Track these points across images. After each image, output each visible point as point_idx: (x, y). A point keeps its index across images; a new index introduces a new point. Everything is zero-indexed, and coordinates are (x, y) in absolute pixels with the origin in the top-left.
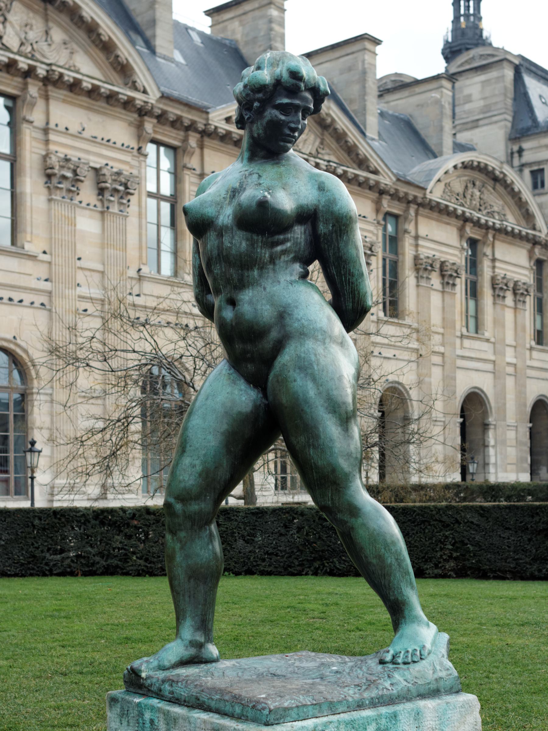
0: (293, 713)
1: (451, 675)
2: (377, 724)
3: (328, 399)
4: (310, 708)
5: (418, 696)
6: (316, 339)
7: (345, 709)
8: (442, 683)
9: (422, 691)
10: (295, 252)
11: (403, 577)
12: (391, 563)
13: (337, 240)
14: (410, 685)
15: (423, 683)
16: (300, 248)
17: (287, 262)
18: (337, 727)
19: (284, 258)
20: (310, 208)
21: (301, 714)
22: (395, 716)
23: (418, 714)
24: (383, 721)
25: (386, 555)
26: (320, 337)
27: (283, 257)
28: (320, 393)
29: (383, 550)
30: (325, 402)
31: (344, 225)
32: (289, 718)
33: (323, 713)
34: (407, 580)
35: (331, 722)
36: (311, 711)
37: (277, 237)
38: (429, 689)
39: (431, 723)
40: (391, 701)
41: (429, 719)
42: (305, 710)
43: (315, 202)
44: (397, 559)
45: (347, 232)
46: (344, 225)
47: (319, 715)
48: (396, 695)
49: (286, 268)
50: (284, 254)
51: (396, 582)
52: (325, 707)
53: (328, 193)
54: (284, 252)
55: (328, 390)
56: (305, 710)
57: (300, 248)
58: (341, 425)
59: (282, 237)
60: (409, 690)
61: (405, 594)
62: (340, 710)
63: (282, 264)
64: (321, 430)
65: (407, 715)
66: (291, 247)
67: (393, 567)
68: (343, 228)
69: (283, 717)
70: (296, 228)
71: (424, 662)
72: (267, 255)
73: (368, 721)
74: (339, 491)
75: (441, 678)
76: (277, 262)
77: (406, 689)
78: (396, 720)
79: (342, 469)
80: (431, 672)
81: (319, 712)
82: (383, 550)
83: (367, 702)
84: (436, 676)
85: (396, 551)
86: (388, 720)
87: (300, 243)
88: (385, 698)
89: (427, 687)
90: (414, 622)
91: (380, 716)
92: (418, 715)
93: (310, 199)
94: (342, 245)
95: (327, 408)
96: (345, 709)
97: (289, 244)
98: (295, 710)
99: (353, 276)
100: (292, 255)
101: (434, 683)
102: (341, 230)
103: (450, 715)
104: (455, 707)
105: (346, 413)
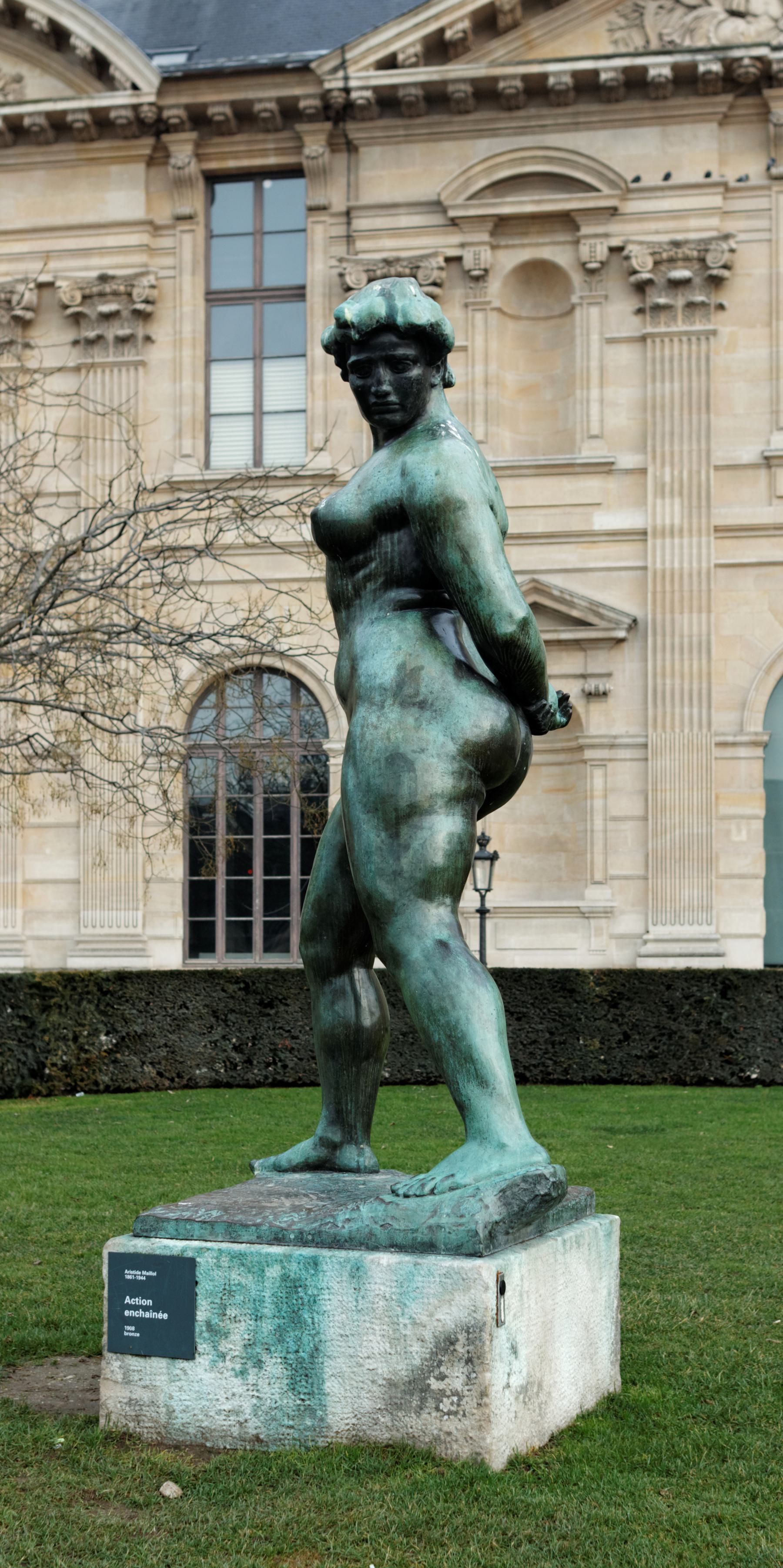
0: (171, 1227)
1: (461, 1225)
2: (283, 1268)
3: (368, 792)
4: (196, 1226)
5: (392, 1246)
6: (372, 704)
7: (254, 1238)
8: (441, 1236)
9: (399, 1239)
10: (386, 573)
11: (461, 1065)
12: (439, 1042)
13: (430, 545)
14: (375, 1226)
15: (403, 1227)
16: (392, 567)
17: (375, 591)
18: (217, 1258)
19: (370, 586)
20: (391, 504)
21: (182, 1231)
22: (315, 1263)
23: (358, 1269)
24: (294, 1267)
25: (432, 1028)
26: (378, 699)
27: (368, 585)
28: (359, 784)
29: (426, 1021)
30: (364, 796)
31: (430, 521)
32: (163, 1233)
33: (217, 1236)
34: (468, 1071)
35: (208, 1249)
36: (197, 1230)
37: (354, 559)
38: (414, 1239)
39: (382, 1288)
40: (336, 1243)
41: (378, 1281)
42: (188, 1227)
43: (398, 495)
44: (449, 1037)
45: (439, 529)
46: (430, 521)
47: (210, 1238)
48: (346, 1235)
49: (374, 601)
50: (370, 580)
51: (450, 1072)
52: (220, 1229)
53: (409, 478)
54: (368, 578)
55: (369, 778)
56: (188, 1227)
57: (392, 567)
58: (386, 829)
59: (361, 557)
60: (371, 1234)
61: (463, 1092)
62: (245, 1239)
63: (368, 596)
64: (356, 837)
65: (337, 1266)
66: (376, 568)
67: (444, 1049)
68: (431, 524)
69: (155, 1230)
70: (383, 538)
71: (431, 1197)
72: (350, 587)
73: (269, 1261)
74: (381, 929)
75: (439, 1227)
76: (363, 593)
77: (367, 1230)
78: (316, 1270)
79: (382, 895)
80: (428, 1214)
81: (211, 1234)
82: (426, 1021)
83: (292, 1236)
84: (432, 1221)
85: (448, 1023)
86: (301, 1266)
87: (392, 560)
88: (324, 1237)
89: (410, 1236)
90: (475, 1138)
91: (288, 1257)
92: (357, 1272)
93: (390, 492)
94: (437, 550)
95: (365, 806)
96: (254, 1238)
97: (373, 565)
98: (173, 1223)
99: (464, 593)
100: (381, 580)
101: (426, 1232)
102: (429, 528)
103: (420, 1284)
104: (430, 1273)
105: (396, 810)
